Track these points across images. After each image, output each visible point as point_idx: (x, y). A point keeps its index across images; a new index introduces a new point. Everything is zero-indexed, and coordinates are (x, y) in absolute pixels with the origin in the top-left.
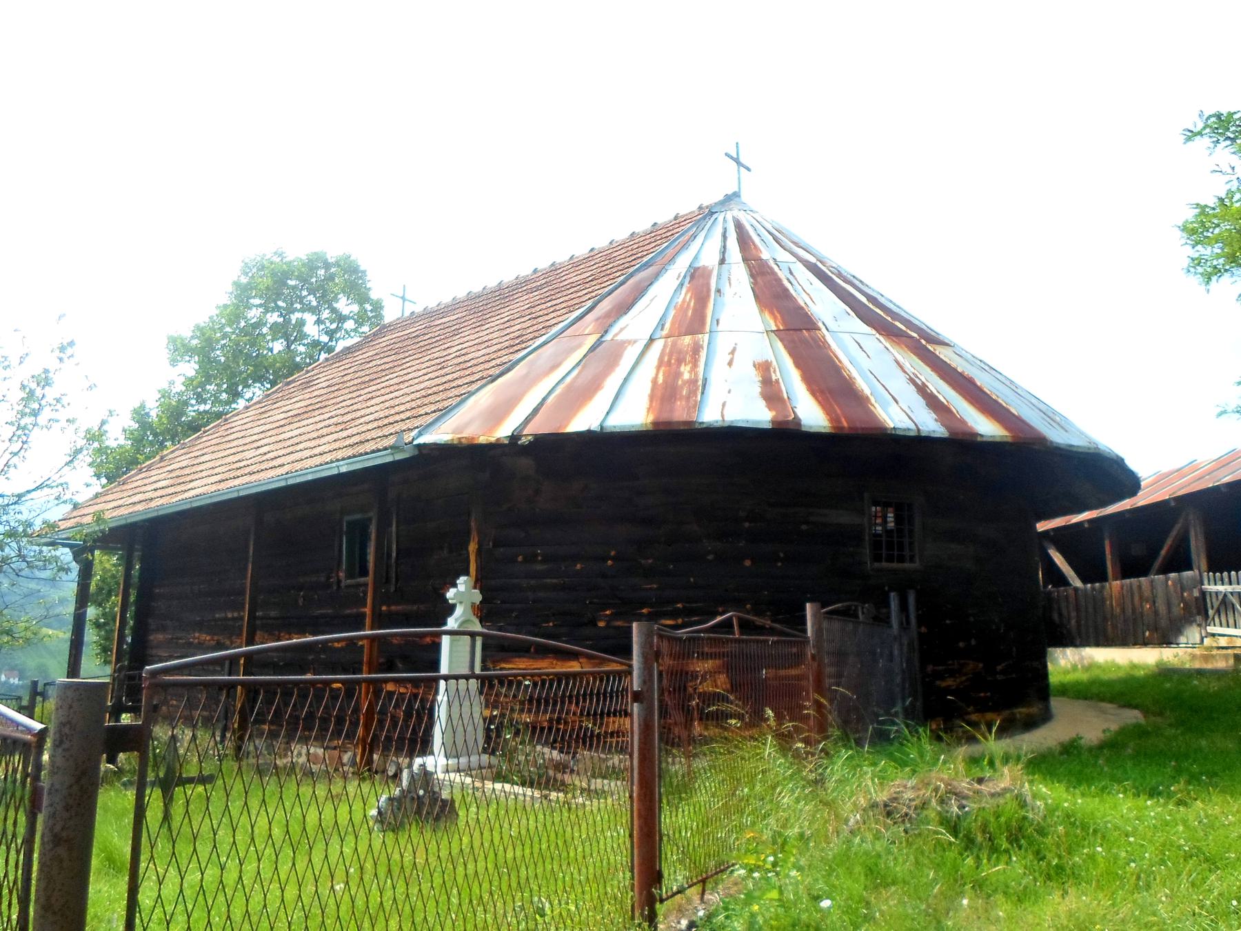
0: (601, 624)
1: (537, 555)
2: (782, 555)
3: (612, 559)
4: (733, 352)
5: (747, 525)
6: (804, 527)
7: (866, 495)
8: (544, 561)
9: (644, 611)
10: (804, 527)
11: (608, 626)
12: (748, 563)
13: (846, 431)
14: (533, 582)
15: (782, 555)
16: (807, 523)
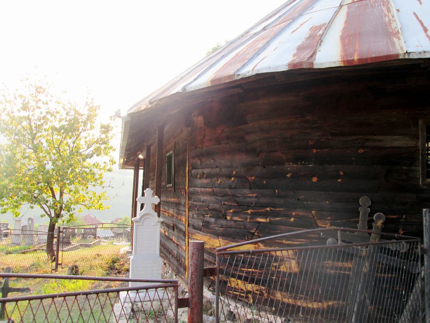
0: (228, 218)
1: (204, 174)
2: (341, 173)
3: (235, 176)
4: (302, 25)
5: (315, 151)
6: (361, 151)
7: (420, 122)
8: (206, 178)
9: (249, 211)
10: (361, 151)
11: (231, 220)
12: (315, 179)
13: (356, 63)
14: (203, 190)
15: (341, 173)
16: (363, 147)
